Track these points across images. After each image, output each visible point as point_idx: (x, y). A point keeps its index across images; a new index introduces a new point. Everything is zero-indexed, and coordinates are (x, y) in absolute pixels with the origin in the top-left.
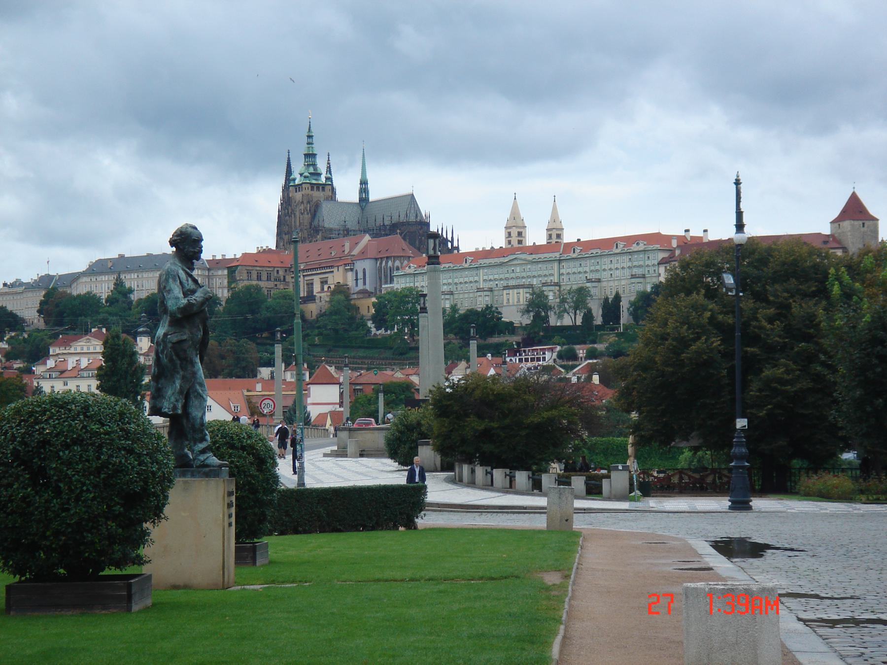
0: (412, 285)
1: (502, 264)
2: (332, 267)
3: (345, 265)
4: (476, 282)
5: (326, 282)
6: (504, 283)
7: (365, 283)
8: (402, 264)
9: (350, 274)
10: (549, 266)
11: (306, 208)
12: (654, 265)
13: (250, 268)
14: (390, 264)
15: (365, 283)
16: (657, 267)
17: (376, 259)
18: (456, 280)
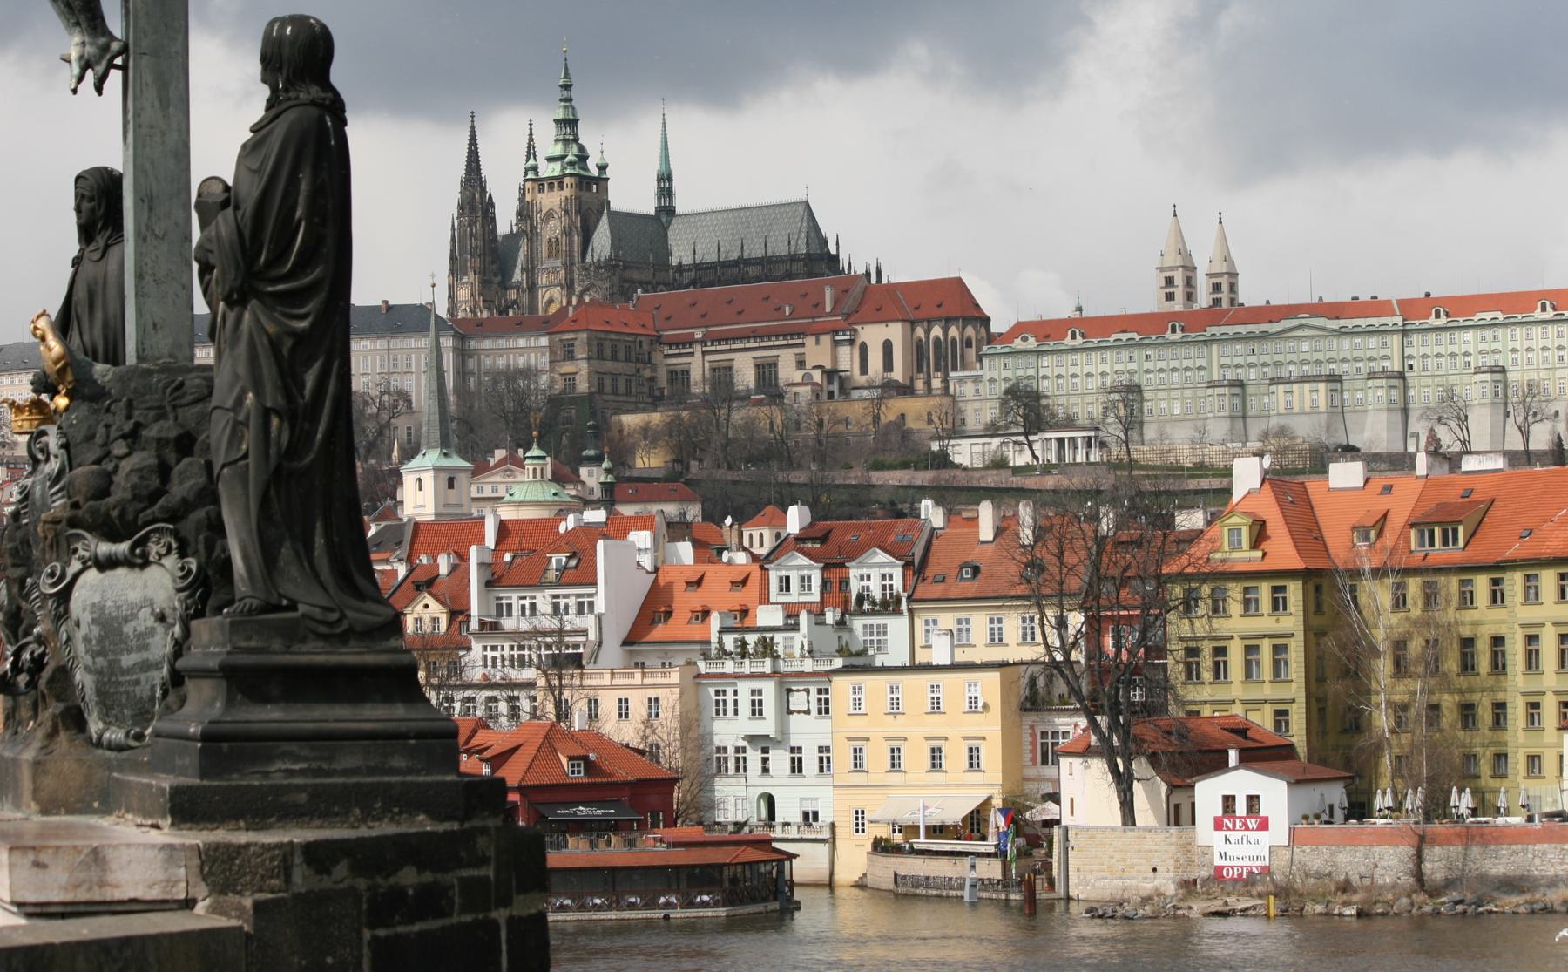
0: (1031, 372)
1: (1265, 336)
2: (799, 335)
3: (836, 332)
4: (1200, 368)
5: (775, 365)
6: (1271, 372)
7: (888, 365)
8: (977, 332)
9: (844, 351)
11: (572, 223)
13: (603, 336)
14: (954, 332)
15: (888, 365)
17: (913, 324)
18: (1147, 365)
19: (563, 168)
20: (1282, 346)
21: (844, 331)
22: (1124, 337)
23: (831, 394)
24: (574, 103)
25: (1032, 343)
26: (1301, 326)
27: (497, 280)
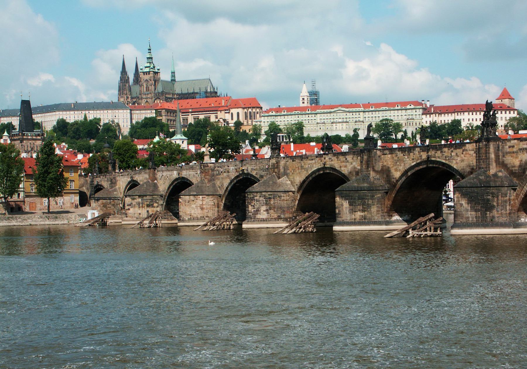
2: (216, 111)
3: (226, 110)
4: (315, 120)
6: (332, 121)
9: (227, 115)
10: (357, 113)
12: (419, 115)
14: (254, 110)
16: (421, 116)
17: (244, 108)
18: (302, 119)
19: (149, 69)
20: (335, 114)
21: (227, 110)
22: (296, 112)
23: (224, 125)
24: (152, 54)
25: (274, 113)
26: (340, 110)
27: (130, 97)
